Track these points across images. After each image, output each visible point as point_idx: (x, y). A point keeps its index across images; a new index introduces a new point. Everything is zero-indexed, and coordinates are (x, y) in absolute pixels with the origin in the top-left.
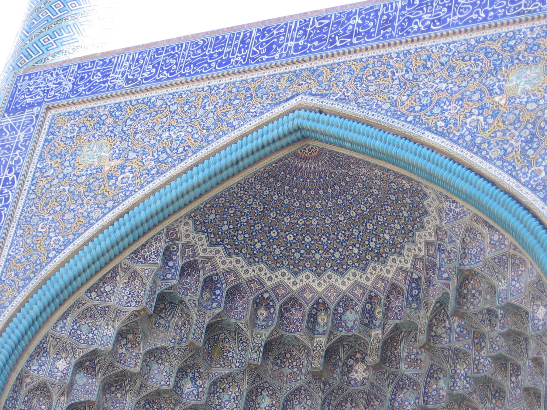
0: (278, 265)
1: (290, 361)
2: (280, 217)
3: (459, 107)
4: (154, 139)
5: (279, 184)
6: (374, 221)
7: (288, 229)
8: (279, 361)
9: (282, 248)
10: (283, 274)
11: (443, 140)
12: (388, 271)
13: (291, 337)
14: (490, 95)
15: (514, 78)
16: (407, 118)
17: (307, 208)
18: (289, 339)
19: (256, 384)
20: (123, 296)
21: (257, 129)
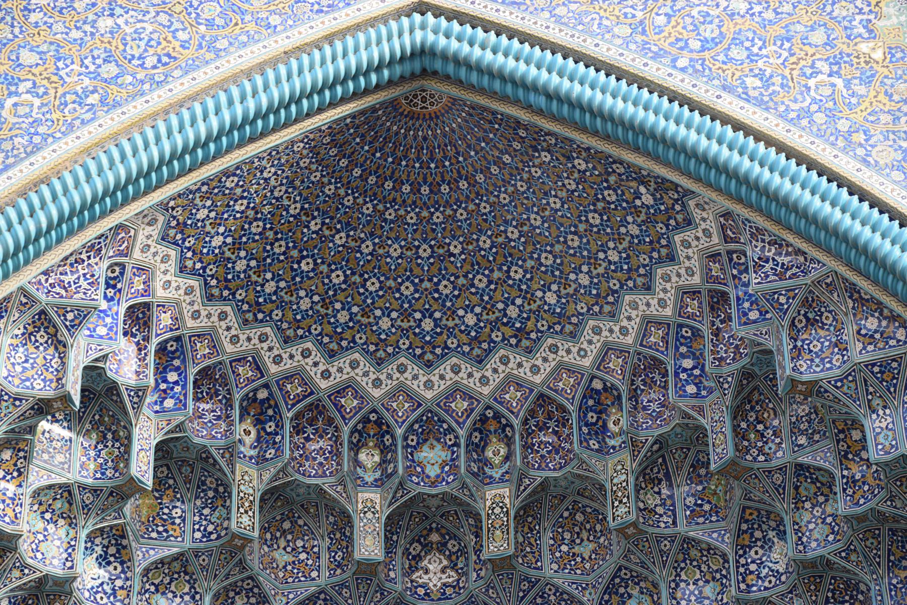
0: (300, 332)
1: (289, 537)
2: (327, 233)
3: (785, 54)
4: (77, 28)
5: (344, 163)
6: (530, 263)
7: (338, 258)
8: (268, 536)
9: (316, 298)
10: (306, 354)
11: (766, 115)
12: (535, 370)
13: (309, 486)
14: (849, 37)
15: (892, 11)
16: (674, 60)
17: (385, 220)
18: (302, 491)
19: (232, 580)
20: (13, 364)
21: (330, 39)
